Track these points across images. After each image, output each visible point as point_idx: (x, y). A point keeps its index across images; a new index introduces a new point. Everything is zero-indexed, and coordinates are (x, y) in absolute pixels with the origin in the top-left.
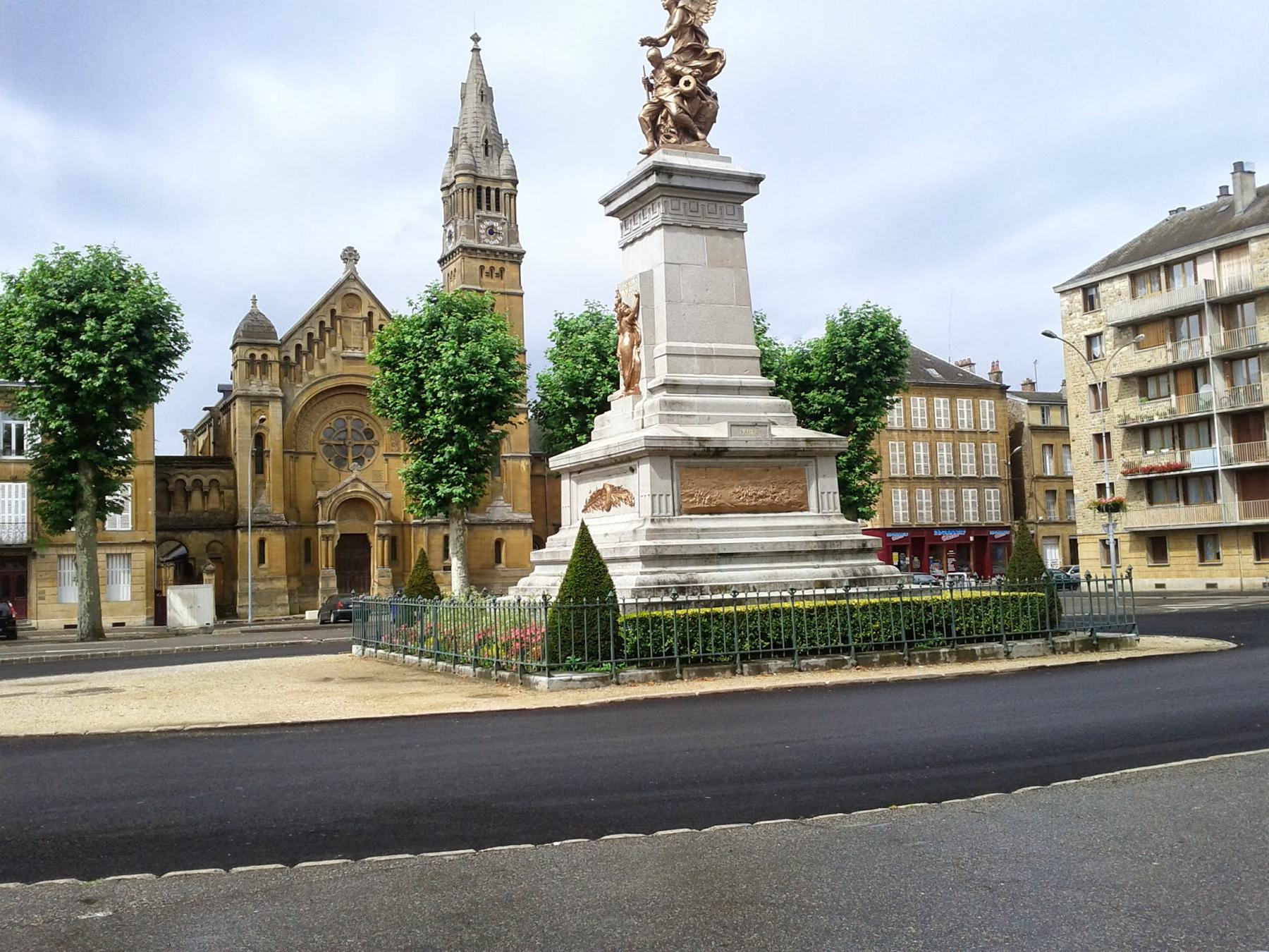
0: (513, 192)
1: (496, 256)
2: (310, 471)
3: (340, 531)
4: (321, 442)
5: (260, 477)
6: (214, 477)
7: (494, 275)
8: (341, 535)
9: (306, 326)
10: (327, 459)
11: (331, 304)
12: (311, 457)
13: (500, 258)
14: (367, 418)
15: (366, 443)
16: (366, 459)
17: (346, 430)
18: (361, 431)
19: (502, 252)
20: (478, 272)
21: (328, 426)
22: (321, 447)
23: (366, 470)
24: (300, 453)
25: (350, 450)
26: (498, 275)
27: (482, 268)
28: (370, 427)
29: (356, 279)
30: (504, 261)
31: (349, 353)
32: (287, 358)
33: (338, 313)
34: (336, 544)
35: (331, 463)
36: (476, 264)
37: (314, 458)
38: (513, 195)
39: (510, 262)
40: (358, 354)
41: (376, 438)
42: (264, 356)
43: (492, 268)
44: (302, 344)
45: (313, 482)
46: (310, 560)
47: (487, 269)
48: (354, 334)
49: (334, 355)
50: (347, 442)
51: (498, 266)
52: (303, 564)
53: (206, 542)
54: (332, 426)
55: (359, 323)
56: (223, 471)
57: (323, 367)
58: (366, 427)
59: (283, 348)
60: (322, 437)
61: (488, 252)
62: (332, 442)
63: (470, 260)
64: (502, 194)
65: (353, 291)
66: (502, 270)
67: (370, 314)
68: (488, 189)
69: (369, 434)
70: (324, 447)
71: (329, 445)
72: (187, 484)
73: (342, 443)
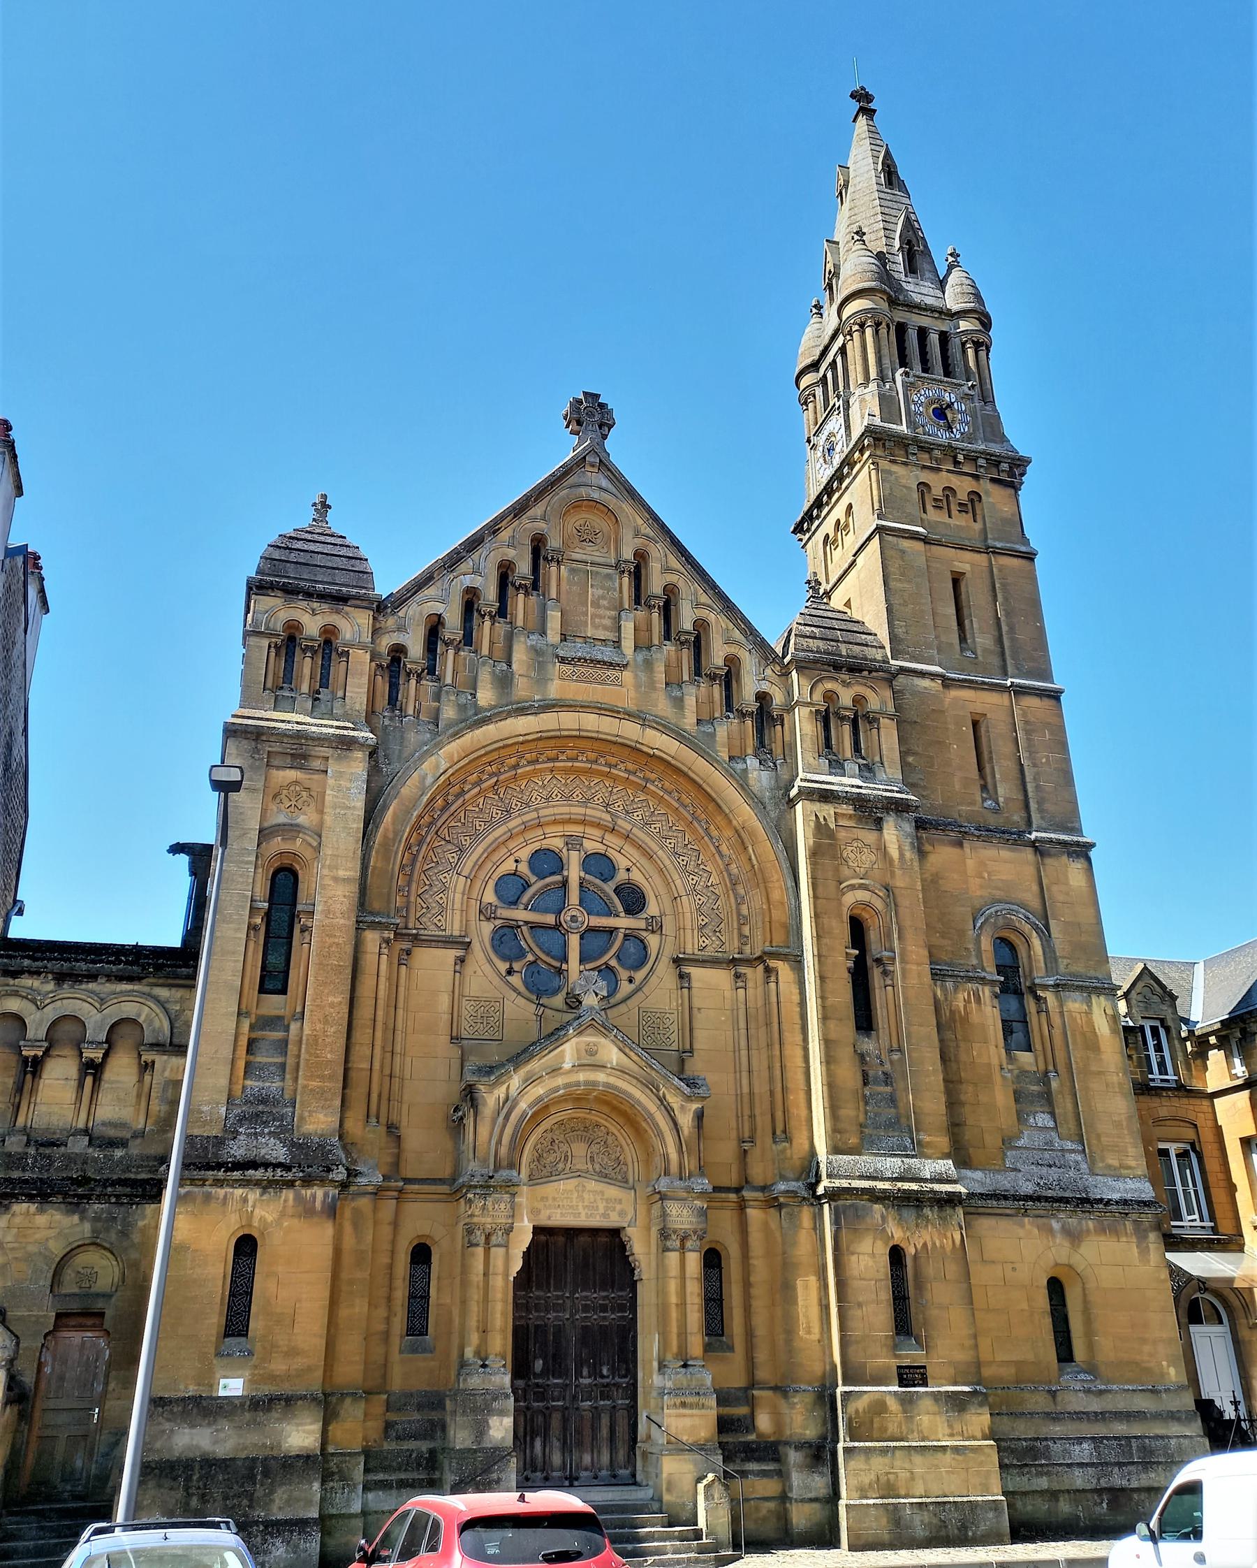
0: (982, 338)
1: (956, 463)
2: (444, 1001)
3: (534, 1212)
4: (486, 913)
5: (274, 1004)
6: (129, 1009)
7: (954, 508)
8: (537, 1230)
9: (463, 567)
10: (503, 967)
11: (534, 519)
12: (452, 954)
13: (965, 470)
14: (628, 848)
15: (623, 922)
16: (623, 974)
17: (565, 884)
18: (609, 888)
19: (972, 458)
20: (916, 496)
21: (509, 866)
22: (487, 928)
23: (623, 1008)
24: (416, 939)
25: (574, 940)
26: (963, 507)
27: (923, 487)
28: (636, 876)
29: (604, 465)
30: (976, 477)
31: (576, 649)
32: (398, 652)
33: (554, 542)
34: (517, 1265)
35: (516, 980)
36: (909, 477)
37: (461, 960)
38: (982, 346)
39: (993, 480)
40: (607, 654)
41: (652, 909)
42: (329, 633)
43: (949, 490)
44: (446, 616)
45: (455, 1039)
46: (423, 1332)
47: (937, 491)
48: (596, 604)
49: (536, 652)
50: (566, 917)
51: (964, 486)
52: (396, 1341)
53: (57, 1249)
54: (524, 868)
55: (608, 576)
56: (163, 993)
57: (504, 682)
58: (621, 876)
59: (391, 622)
60: (490, 897)
61: (937, 453)
62: (520, 914)
63: (894, 468)
64: (955, 343)
65: (596, 495)
66: (975, 497)
67: (641, 557)
68: (923, 333)
69: (633, 900)
70: (495, 932)
71: (511, 927)
72: (30, 1034)
73: (550, 919)
